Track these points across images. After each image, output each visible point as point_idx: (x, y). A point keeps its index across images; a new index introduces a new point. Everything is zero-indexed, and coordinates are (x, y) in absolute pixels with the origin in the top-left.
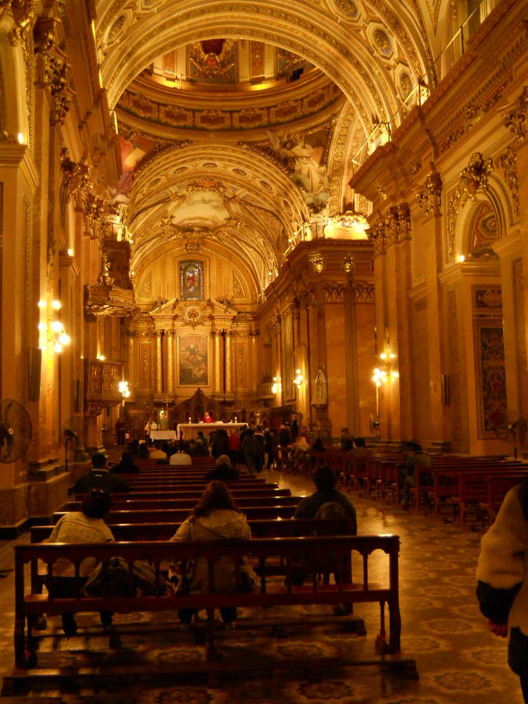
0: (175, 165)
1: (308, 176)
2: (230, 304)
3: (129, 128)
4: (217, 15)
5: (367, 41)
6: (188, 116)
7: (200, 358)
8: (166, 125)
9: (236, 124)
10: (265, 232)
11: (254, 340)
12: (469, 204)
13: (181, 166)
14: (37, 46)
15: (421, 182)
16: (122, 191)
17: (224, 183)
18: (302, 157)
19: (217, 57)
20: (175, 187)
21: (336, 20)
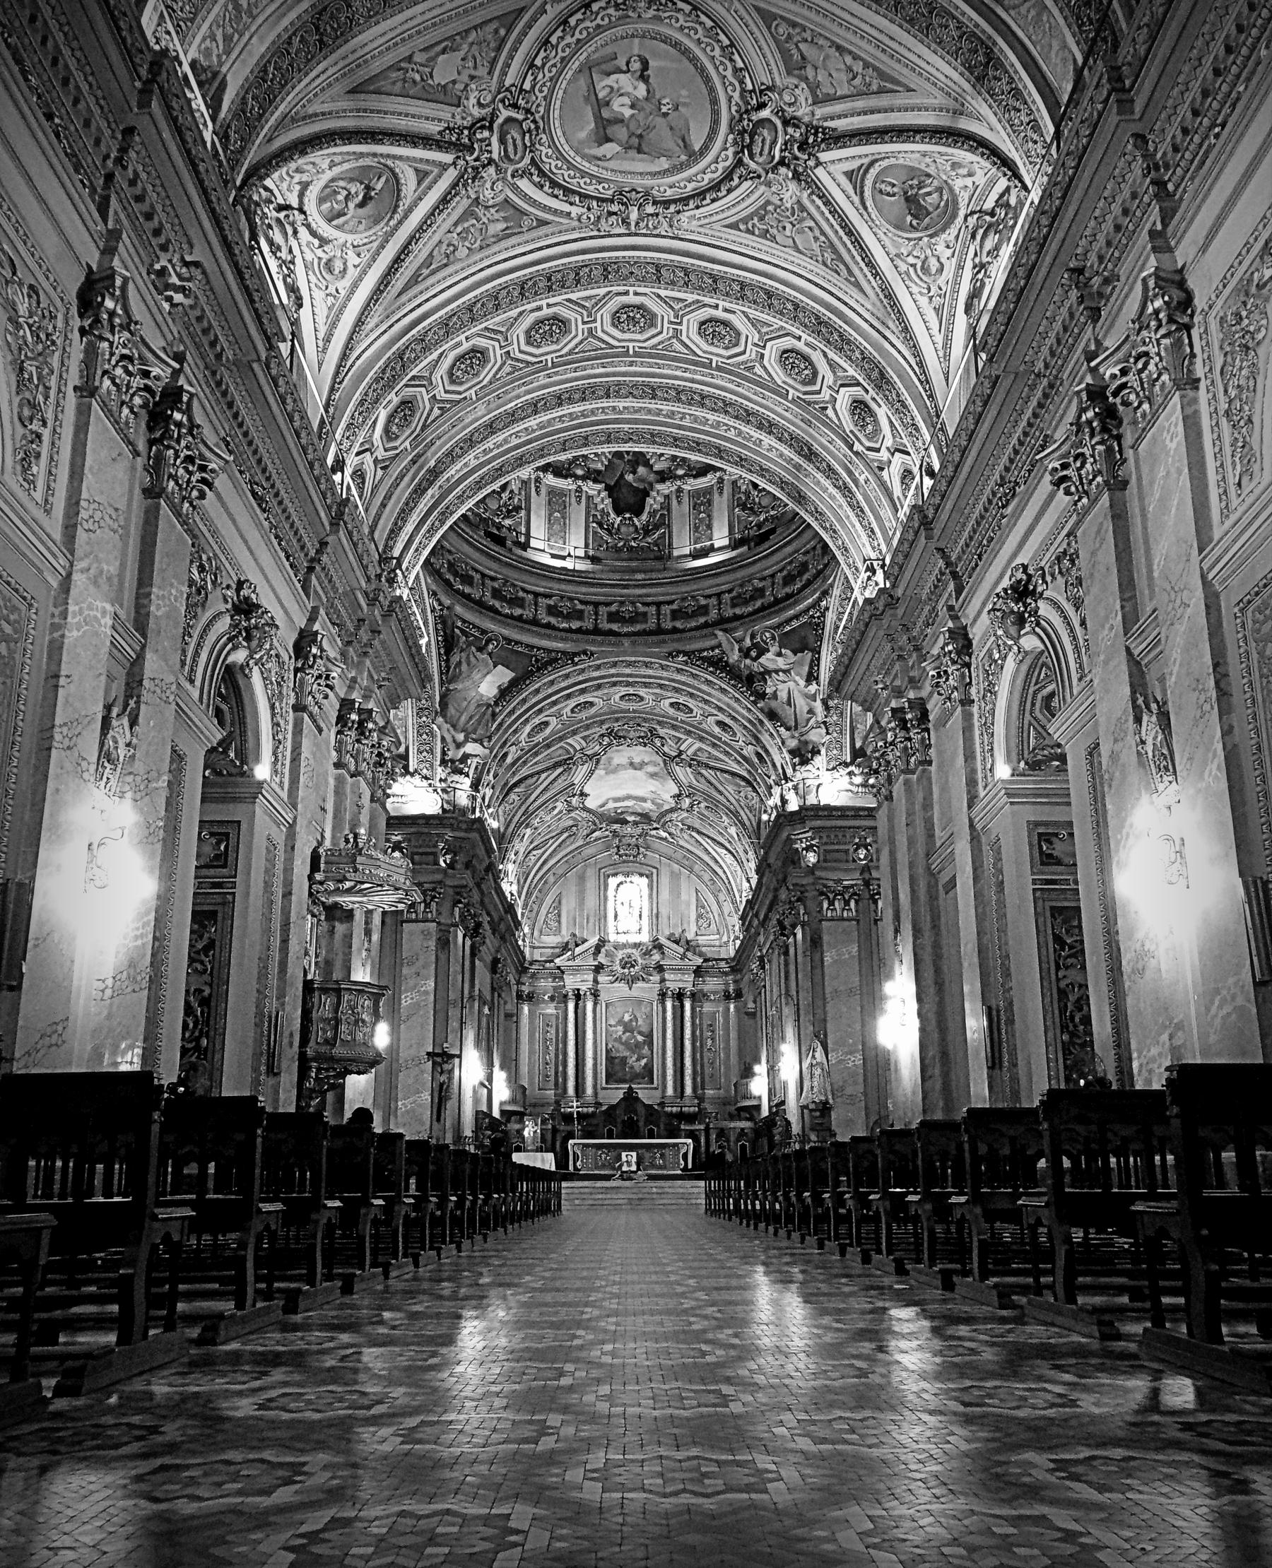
0: (569, 696)
1: (789, 703)
2: (690, 946)
3: (484, 632)
4: (587, 406)
5: (841, 426)
7: (640, 1038)
8: (548, 626)
9: (668, 625)
10: (736, 814)
11: (732, 1007)
12: (1010, 665)
13: (582, 699)
14: (87, 323)
15: (935, 651)
17: (662, 732)
18: (777, 672)
20: (577, 737)
21: (785, 396)
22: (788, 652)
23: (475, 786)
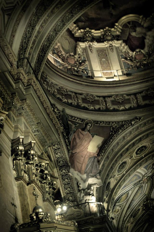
0: (134, 144)
3: (83, 120)
6: (131, 99)
8: (114, 110)
16: (91, 174)
19: (142, 51)
23: (99, 199)
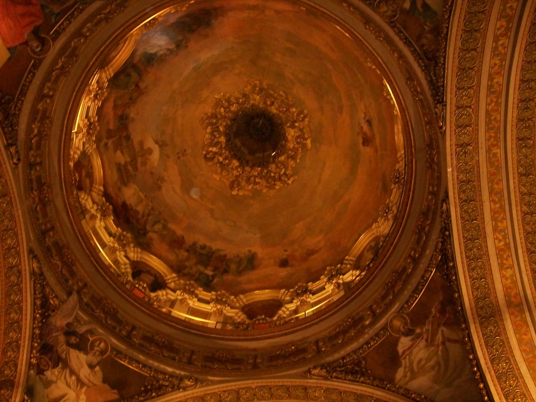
18: (72, 372)
22: (100, 375)
